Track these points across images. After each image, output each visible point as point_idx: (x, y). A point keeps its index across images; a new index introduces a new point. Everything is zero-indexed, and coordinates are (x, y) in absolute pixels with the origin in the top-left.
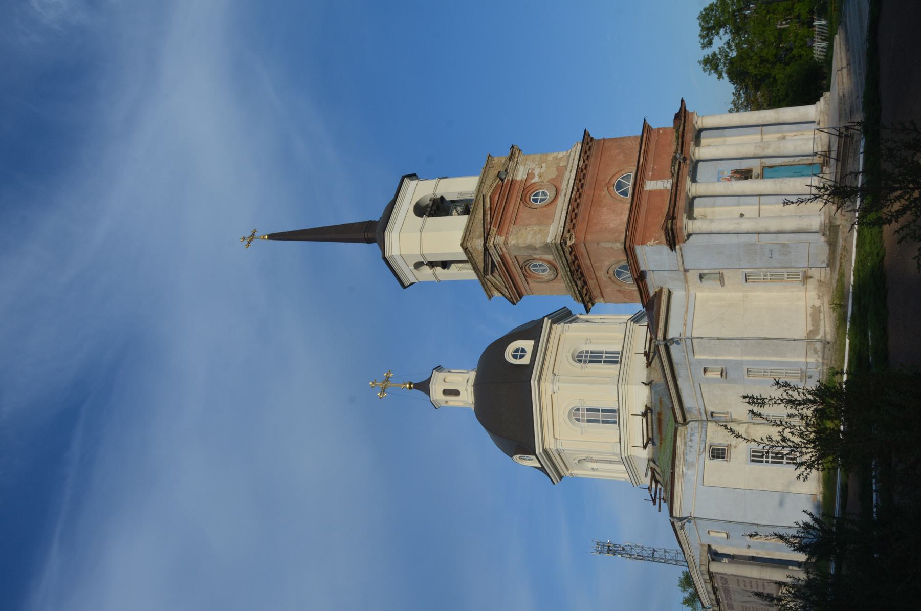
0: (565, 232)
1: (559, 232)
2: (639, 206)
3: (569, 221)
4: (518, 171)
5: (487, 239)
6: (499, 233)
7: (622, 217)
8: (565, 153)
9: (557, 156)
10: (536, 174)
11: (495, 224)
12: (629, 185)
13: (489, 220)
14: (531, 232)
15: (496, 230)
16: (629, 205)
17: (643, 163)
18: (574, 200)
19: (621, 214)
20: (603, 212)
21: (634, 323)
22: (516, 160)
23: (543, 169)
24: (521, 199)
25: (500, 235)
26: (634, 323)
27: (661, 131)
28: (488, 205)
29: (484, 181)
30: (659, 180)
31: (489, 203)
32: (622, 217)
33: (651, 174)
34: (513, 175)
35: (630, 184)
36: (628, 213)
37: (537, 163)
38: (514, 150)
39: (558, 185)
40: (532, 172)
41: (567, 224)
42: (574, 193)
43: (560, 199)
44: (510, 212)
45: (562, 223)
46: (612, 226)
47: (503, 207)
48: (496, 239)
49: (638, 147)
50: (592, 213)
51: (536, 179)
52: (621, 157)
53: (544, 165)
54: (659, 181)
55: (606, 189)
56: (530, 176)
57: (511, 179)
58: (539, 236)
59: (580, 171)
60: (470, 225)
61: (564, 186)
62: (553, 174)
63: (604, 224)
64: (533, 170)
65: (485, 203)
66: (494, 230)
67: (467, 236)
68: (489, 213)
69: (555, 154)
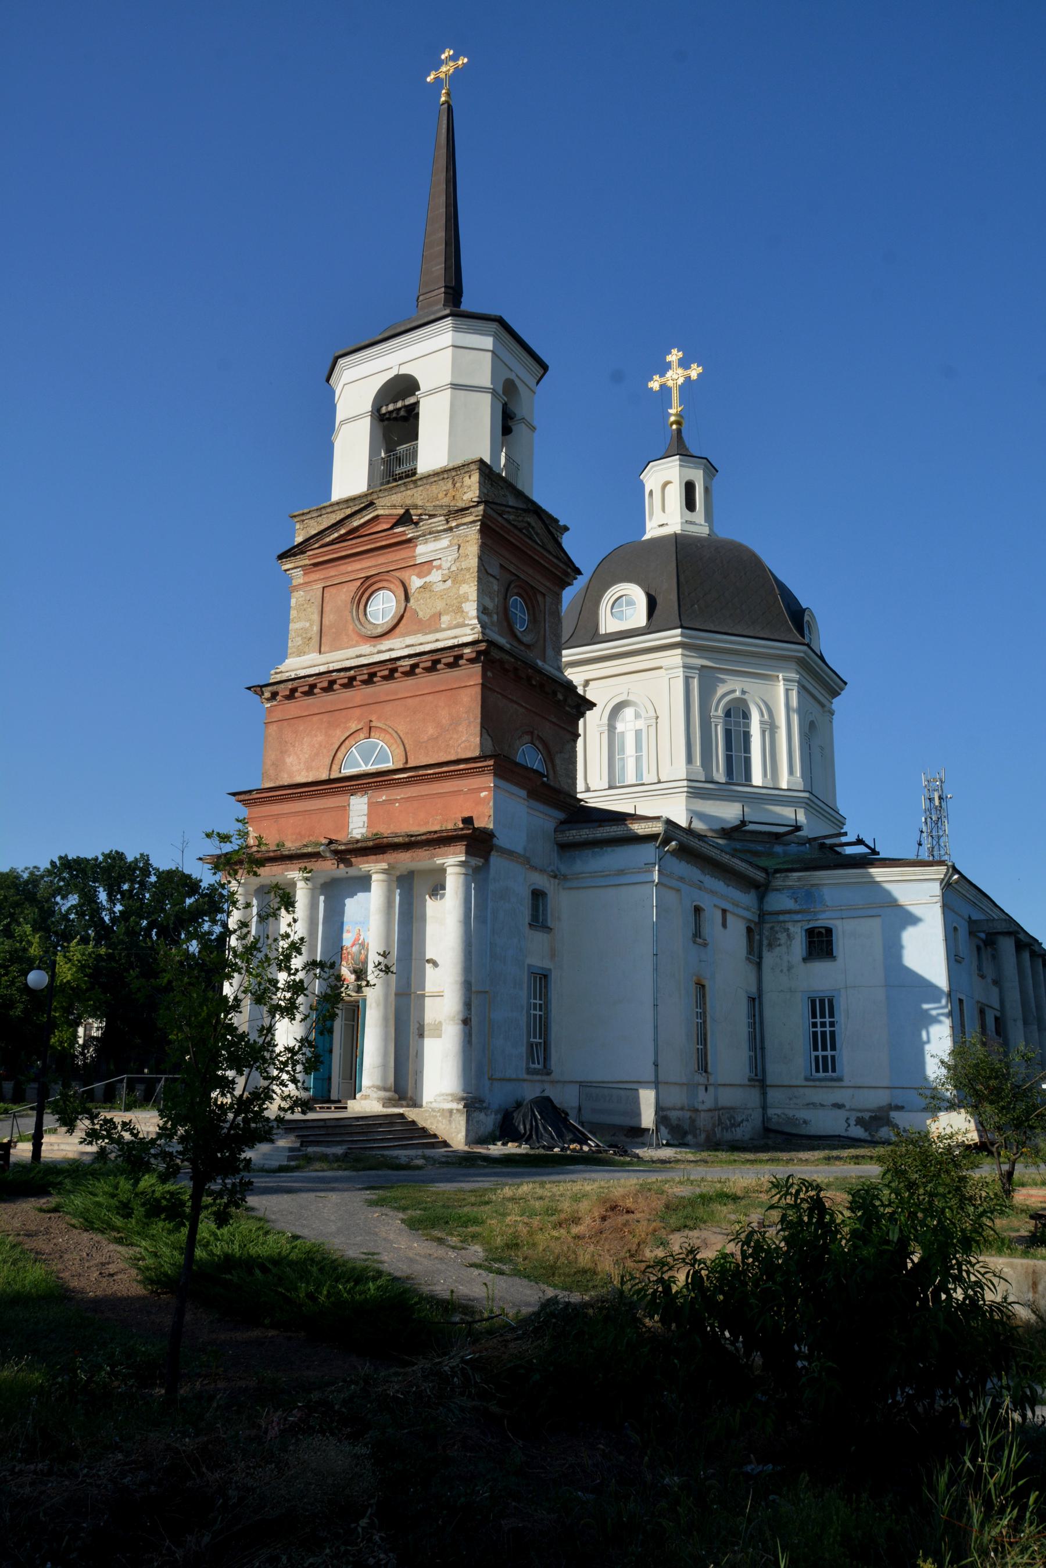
0: (270, 688)
1: (287, 674)
2: (301, 797)
3: (290, 685)
4: (436, 539)
5: (290, 556)
6: (307, 569)
7: (303, 773)
8: (474, 613)
9: (468, 600)
10: (428, 579)
11: (315, 556)
12: (366, 766)
13: (328, 540)
14: (308, 624)
15: (307, 562)
16: (324, 776)
17: (396, 779)
18: (330, 678)
19: (308, 769)
20: (316, 736)
21: (687, 792)
22: (454, 524)
23: (441, 586)
24: (368, 578)
25: (305, 574)
26: (687, 792)
27: (483, 794)
28: (356, 524)
29: (419, 483)
30: (369, 819)
31: (362, 521)
32: (304, 773)
33: (384, 798)
34: (420, 536)
35: (369, 767)
36: (310, 780)
37: (454, 568)
38: (472, 510)
39: (397, 630)
40: (435, 567)
41: (282, 686)
42: (342, 674)
43: (365, 648)
44: (350, 569)
45: (302, 673)
46: (289, 760)
47: (343, 554)
48: (295, 570)
49: (453, 758)
50: (315, 718)
51: (415, 582)
52: (431, 731)
53: (449, 582)
54: (365, 819)
55: (359, 727)
56: (426, 567)
57: (409, 536)
58: (299, 641)
59: (390, 666)
60: (329, 510)
61: (386, 644)
62: (424, 613)
63: (294, 746)
64: (439, 567)
65: (359, 516)
66: (304, 560)
67: (309, 516)
68: (343, 531)
69: (473, 594)
